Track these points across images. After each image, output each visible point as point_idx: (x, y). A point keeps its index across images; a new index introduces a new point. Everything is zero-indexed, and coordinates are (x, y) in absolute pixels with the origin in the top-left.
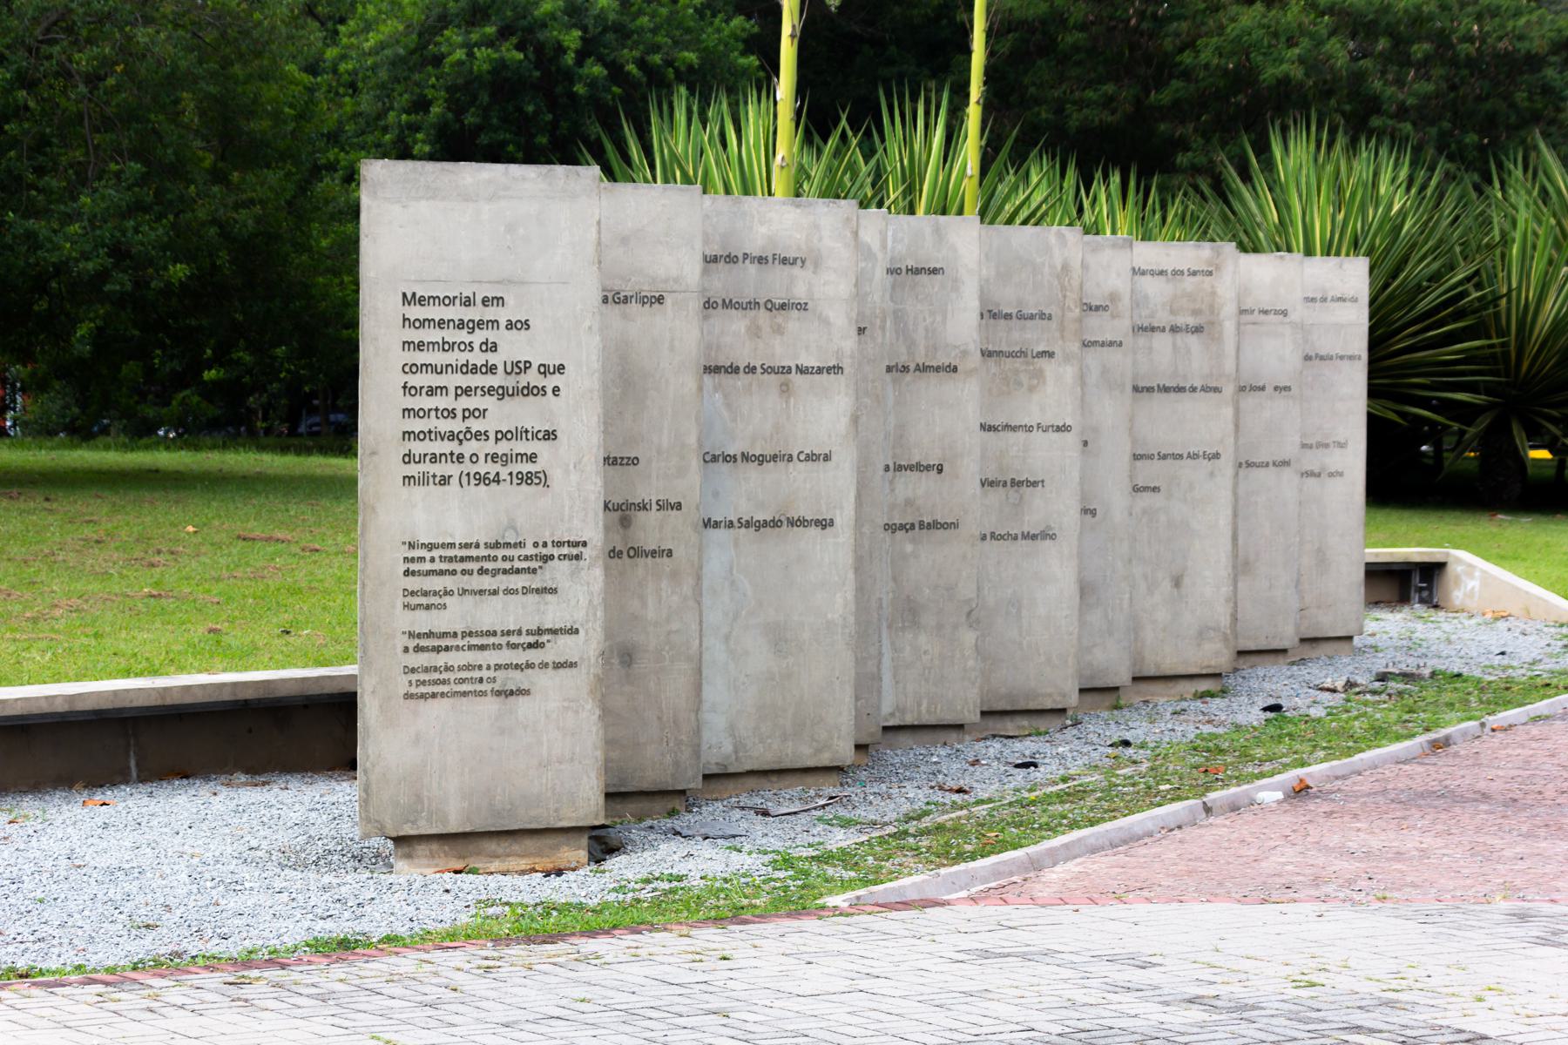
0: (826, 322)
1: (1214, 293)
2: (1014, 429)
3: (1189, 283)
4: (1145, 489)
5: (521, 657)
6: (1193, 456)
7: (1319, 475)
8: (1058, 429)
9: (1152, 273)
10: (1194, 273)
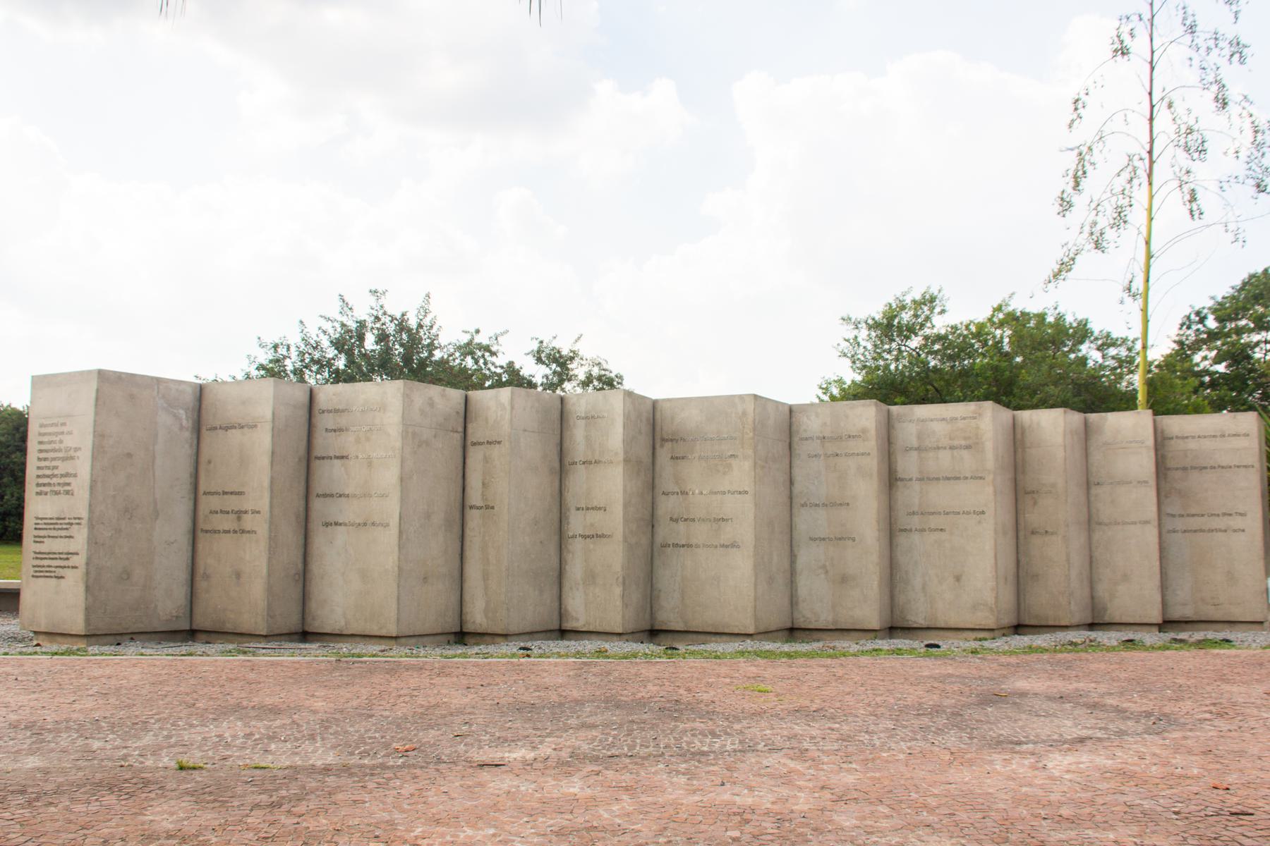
1: (978, 428)
4: (936, 530)
6: (968, 513)
9: (937, 420)
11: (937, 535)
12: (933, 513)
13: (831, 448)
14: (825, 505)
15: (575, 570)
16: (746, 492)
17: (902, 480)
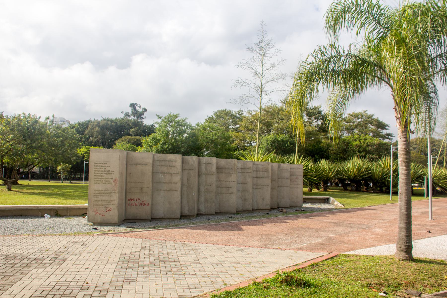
0: (177, 168)
3: (265, 166)
5: (108, 203)
13: (243, 171)
15: (202, 199)
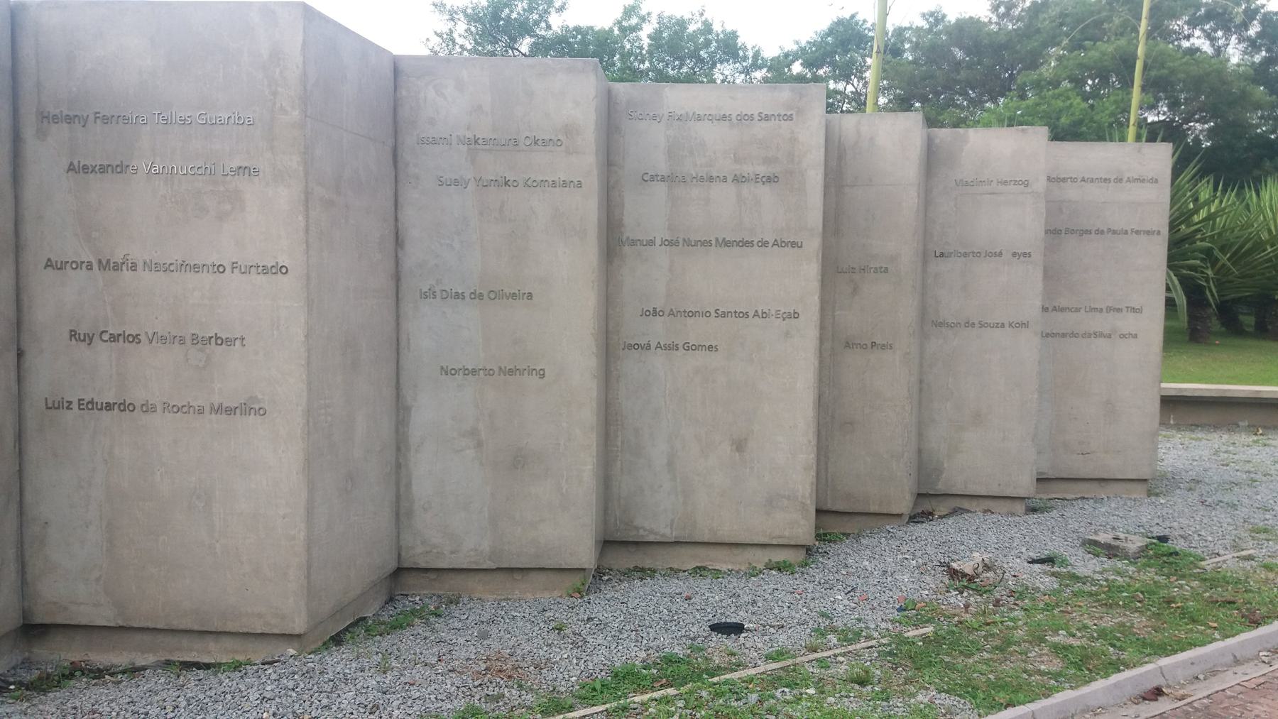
2: (196, 268)
3: (760, 129)
6: (765, 315)
7: (1109, 336)
8: (266, 270)
9: (711, 118)
10: (767, 118)
11: (699, 359)
12: (693, 314)
14: (477, 296)
16: (283, 270)
17: (633, 243)
